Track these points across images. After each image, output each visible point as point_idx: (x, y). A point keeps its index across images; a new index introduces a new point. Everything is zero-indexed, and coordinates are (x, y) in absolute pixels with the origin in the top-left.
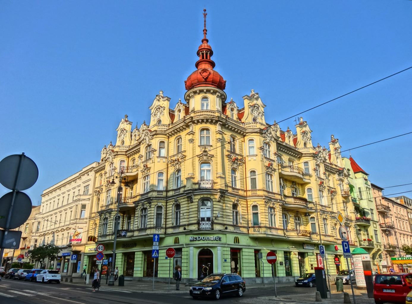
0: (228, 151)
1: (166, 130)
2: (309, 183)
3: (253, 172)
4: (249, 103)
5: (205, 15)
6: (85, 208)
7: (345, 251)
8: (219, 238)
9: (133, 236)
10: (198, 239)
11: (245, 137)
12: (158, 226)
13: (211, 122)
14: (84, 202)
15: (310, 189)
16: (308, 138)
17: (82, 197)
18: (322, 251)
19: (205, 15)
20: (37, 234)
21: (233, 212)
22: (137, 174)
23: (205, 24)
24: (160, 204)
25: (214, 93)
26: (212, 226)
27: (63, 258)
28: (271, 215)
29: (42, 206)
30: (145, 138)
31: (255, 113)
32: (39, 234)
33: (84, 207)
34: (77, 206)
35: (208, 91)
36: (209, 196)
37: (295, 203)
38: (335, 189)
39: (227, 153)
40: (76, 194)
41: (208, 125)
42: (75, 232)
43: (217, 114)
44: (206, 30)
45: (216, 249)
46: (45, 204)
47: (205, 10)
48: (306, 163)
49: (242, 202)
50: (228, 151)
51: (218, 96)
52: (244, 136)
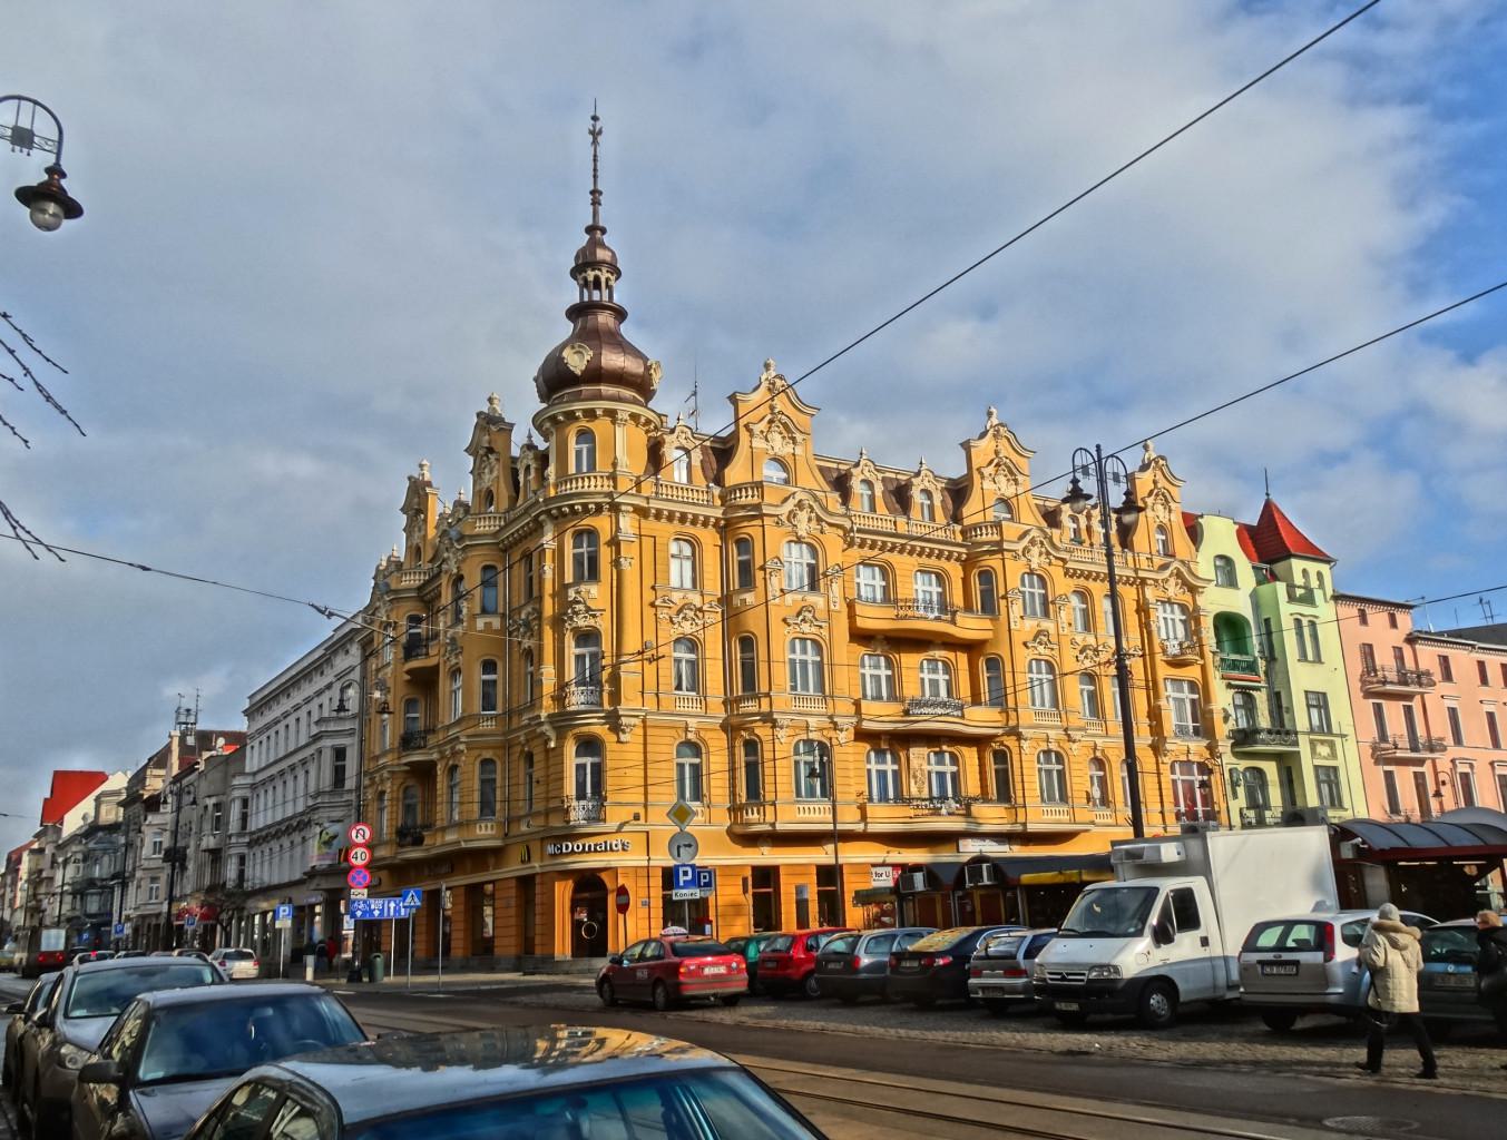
1: (498, 528)
5: (595, 134)
6: (344, 760)
7: (681, 884)
8: (623, 845)
9: (434, 846)
10: (564, 851)
14: (339, 742)
17: (332, 727)
18: (707, 880)
19: (595, 134)
20: (240, 840)
21: (681, 766)
22: (437, 666)
23: (595, 170)
24: (488, 754)
27: (307, 911)
29: (248, 748)
30: (446, 555)
32: (247, 840)
33: (340, 753)
34: (321, 752)
40: (315, 717)
42: (321, 833)
46: (256, 743)
47: (595, 118)
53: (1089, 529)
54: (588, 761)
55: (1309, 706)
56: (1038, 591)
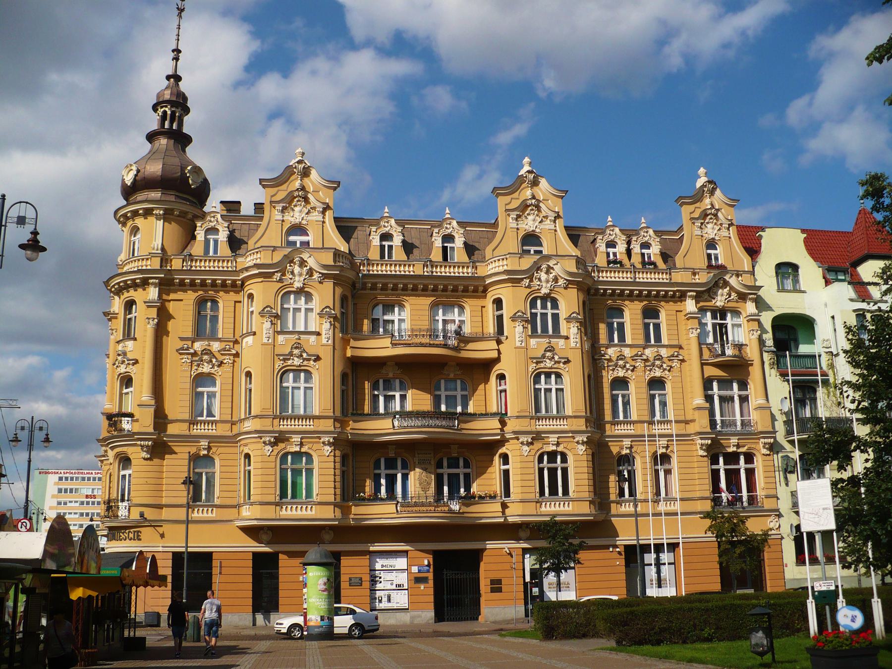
0: (182, 339)
2: (497, 360)
3: (249, 374)
4: (272, 196)
13: (135, 285)
16: (546, 217)
25: (148, 213)
28: (296, 473)
31: (297, 215)
35: (135, 213)
37: (405, 427)
38: (681, 347)
39: (180, 344)
41: (132, 294)
44: (179, 51)
48: (498, 303)
49: (221, 450)
50: (182, 339)
51: (158, 218)
53: (629, 252)
56: (550, 312)
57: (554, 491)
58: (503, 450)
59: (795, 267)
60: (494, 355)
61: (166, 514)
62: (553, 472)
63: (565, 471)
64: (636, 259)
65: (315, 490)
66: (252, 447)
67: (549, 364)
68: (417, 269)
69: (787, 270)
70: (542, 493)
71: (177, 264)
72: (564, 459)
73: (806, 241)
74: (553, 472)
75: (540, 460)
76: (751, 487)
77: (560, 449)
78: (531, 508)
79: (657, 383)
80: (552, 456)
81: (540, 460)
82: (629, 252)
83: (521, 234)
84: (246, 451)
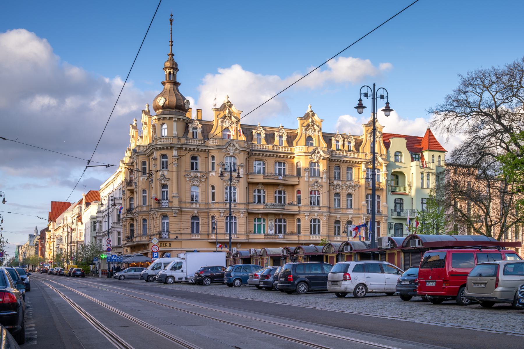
3: (213, 188)
11: (210, 154)
12: (144, 234)
15: (299, 192)
24: (144, 217)
26: (168, 235)
36: (166, 213)
43: (175, 141)
45: (172, 253)
52: (208, 152)
53: (343, 145)
54: (166, 221)
55: (422, 203)
57: (315, 233)
58: (298, 217)
59: (400, 152)
60: (297, 183)
61: (183, 237)
62: (315, 226)
63: (319, 225)
64: (346, 148)
65: (238, 230)
66: (215, 214)
67: (316, 187)
68: (270, 147)
69: (398, 154)
70: (311, 233)
71: (183, 141)
72: (319, 222)
73: (407, 143)
74: (315, 226)
75: (311, 222)
76: (379, 234)
77: (318, 218)
78: (307, 238)
79: (350, 195)
80: (315, 220)
81: (311, 222)
82: (343, 145)
83: (307, 136)
84: (212, 214)
